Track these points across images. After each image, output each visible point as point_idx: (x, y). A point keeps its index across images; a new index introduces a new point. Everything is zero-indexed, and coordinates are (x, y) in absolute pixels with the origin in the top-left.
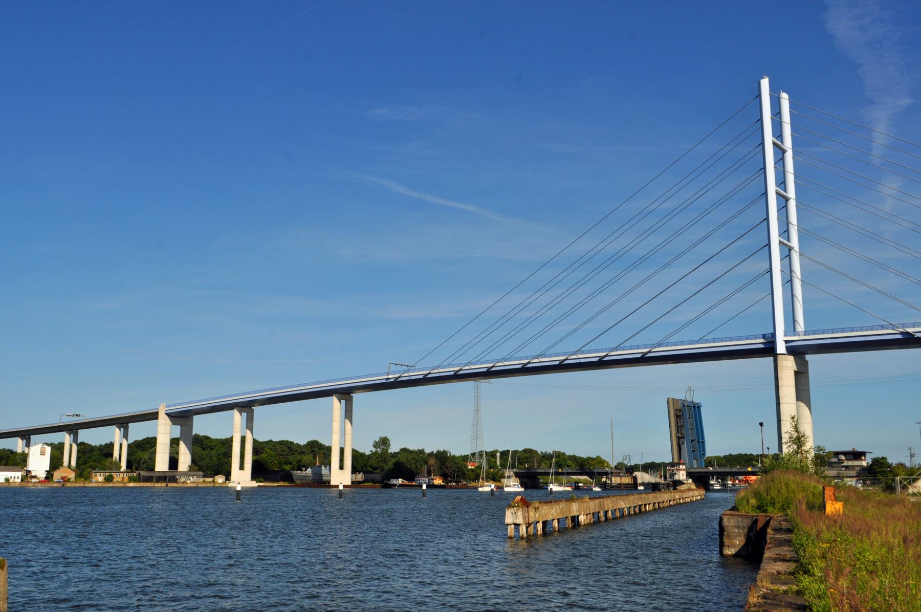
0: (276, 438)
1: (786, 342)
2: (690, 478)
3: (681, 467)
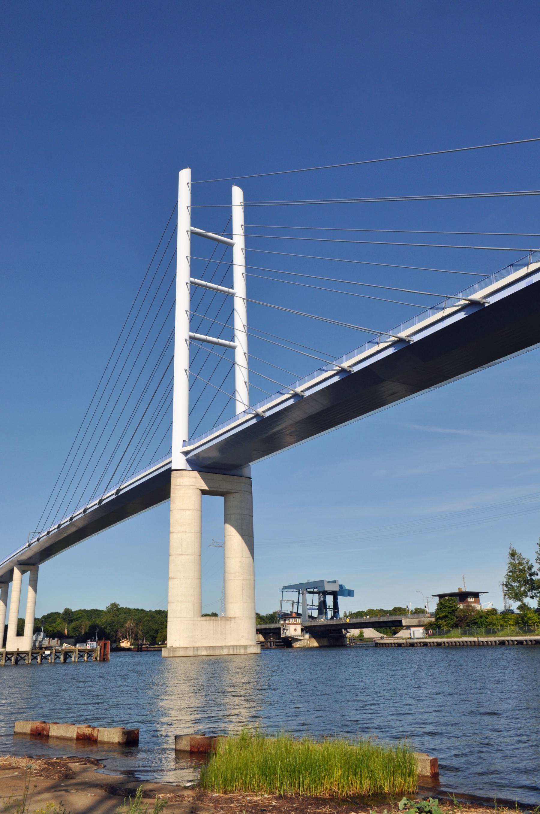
0: (89, 608)
1: (186, 453)
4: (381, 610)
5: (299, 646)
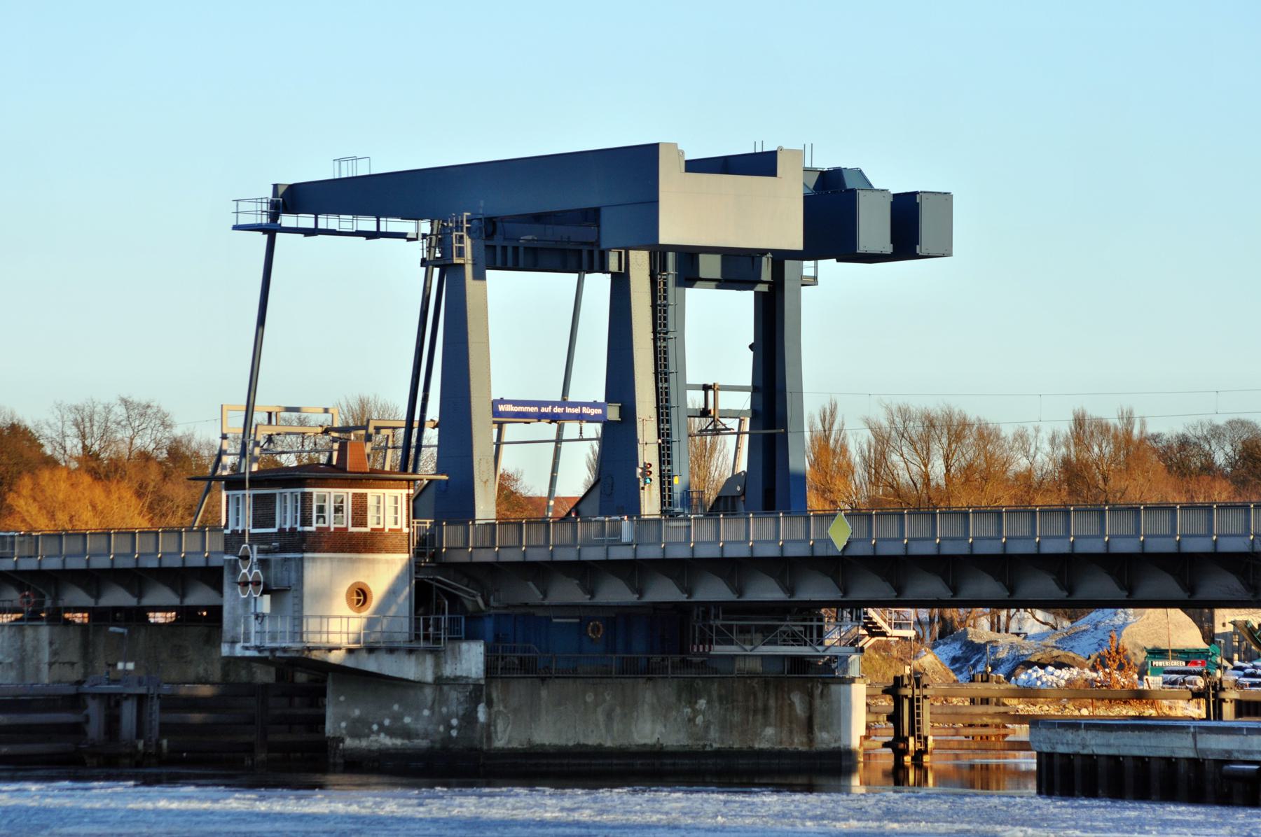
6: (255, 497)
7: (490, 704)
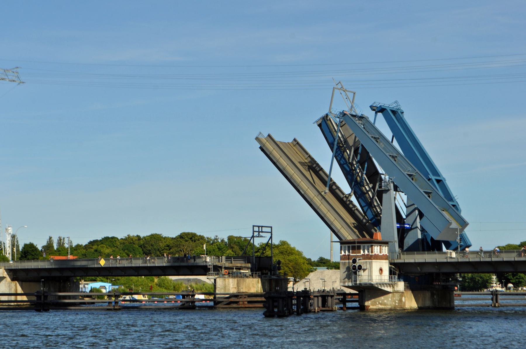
2: (399, 278)
3: (376, 249)
4: (106, 239)
5: (380, 307)
6: (352, 246)
7: (405, 298)
